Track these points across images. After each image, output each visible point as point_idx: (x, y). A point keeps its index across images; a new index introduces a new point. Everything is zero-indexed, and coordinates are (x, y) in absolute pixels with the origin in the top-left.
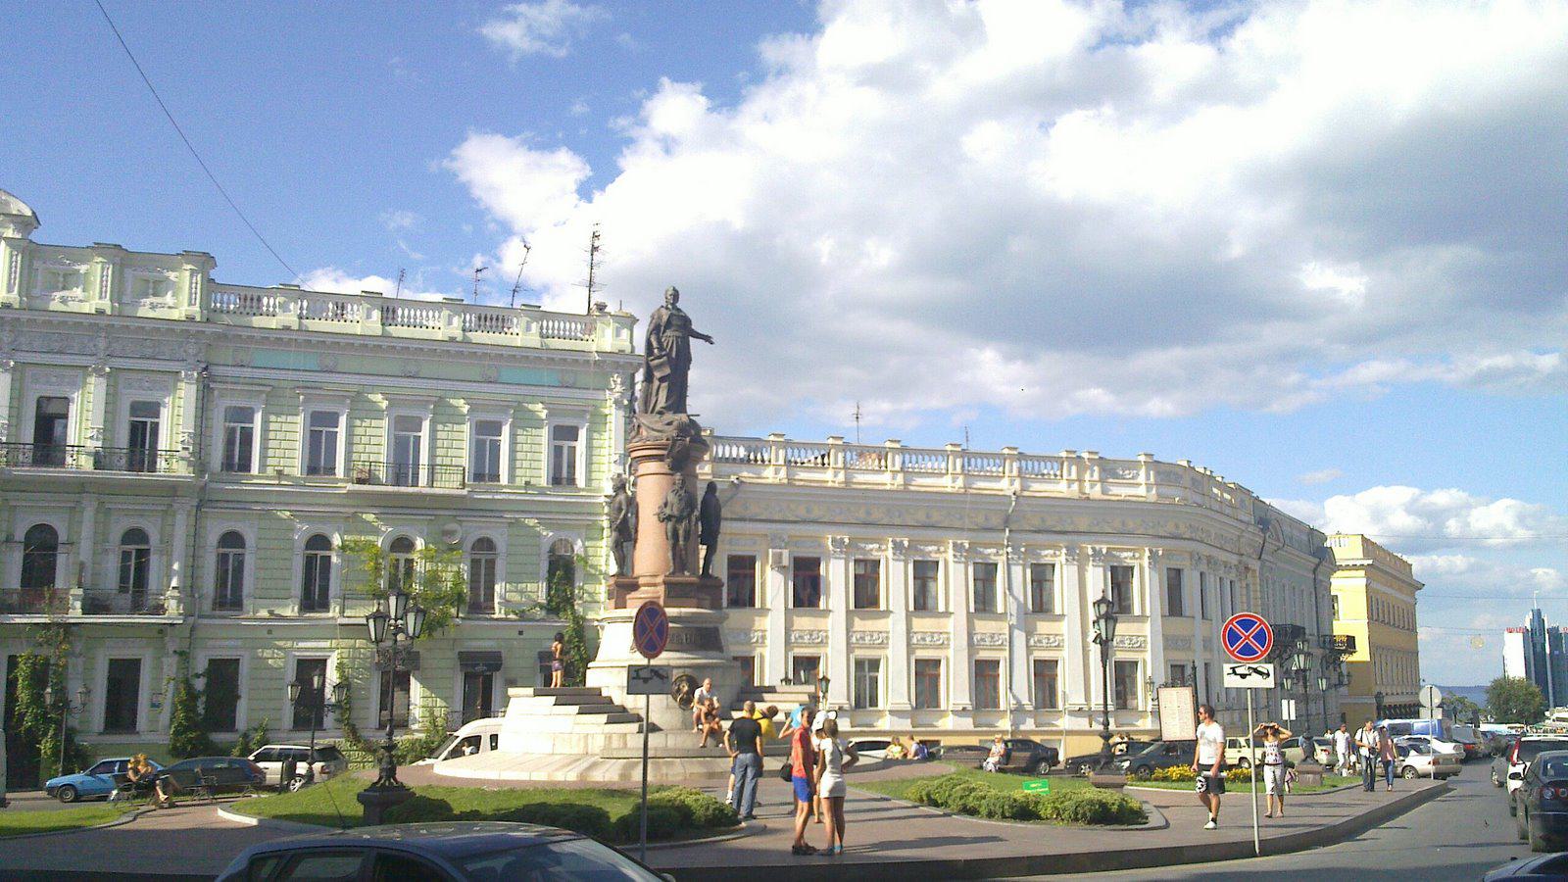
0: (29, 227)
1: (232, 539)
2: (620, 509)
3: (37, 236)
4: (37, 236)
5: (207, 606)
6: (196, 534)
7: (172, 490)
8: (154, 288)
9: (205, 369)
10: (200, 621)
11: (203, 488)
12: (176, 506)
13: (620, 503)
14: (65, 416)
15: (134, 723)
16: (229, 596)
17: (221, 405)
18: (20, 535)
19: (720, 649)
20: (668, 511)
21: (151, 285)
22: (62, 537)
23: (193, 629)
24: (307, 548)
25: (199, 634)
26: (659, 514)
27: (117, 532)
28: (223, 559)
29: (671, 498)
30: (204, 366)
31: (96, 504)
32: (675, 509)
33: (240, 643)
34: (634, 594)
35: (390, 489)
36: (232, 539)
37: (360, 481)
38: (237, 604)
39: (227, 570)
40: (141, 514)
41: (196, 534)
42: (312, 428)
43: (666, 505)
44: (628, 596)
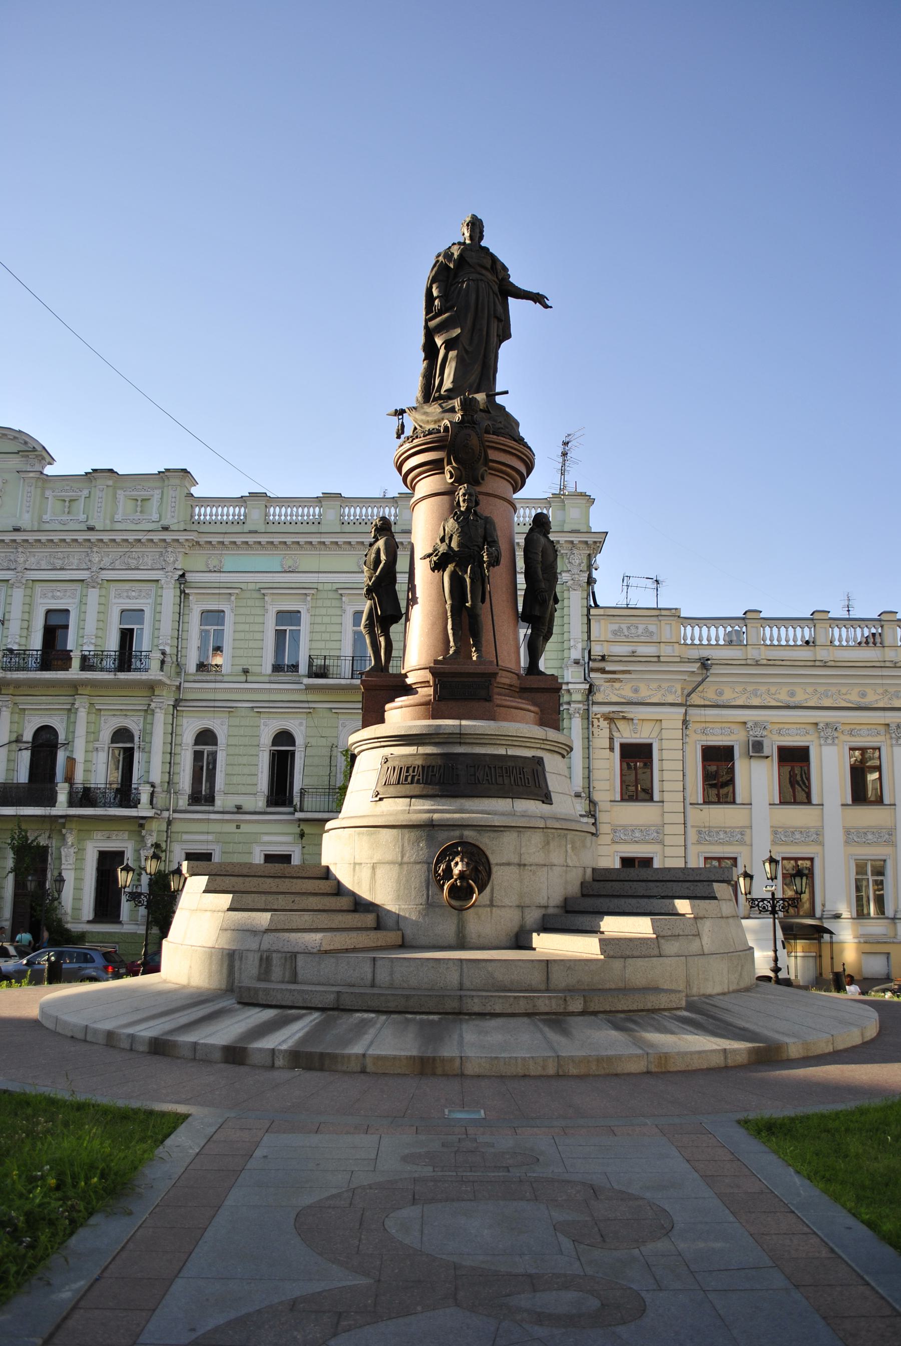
0: (43, 462)
1: (206, 737)
2: (377, 561)
3: (49, 470)
4: (49, 470)
5: (183, 802)
6: (173, 733)
7: (151, 687)
8: (141, 506)
9: (183, 576)
10: (176, 815)
11: (179, 688)
12: (153, 705)
13: (378, 550)
14: (66, 627)
15: (119, 916)
16: (203, 793)
17: (196, 608)
18: (28, 736)
19: (546, 798)
20: (443, 548)
21: (139, 503)
22: (62, 738)
23: (169, 823)
24: (274, 744)
25: (175, 827)
26: (429, 556)
27: (106, 735)
28: (198, 756)
29: (451, 525)
30: (181, 573)
31: (87, 705)
32: (454, 545)
33: (210, 837)
34: (400, 701)
35: (348, 681)
36: (206, 737)
37: (318, 676)
38: (210, 799)
39: (202, 767)
40: (124, 713)
41: (173, 733)
42: (278, 628)
43: (442, 540)
44: (387, 706)
